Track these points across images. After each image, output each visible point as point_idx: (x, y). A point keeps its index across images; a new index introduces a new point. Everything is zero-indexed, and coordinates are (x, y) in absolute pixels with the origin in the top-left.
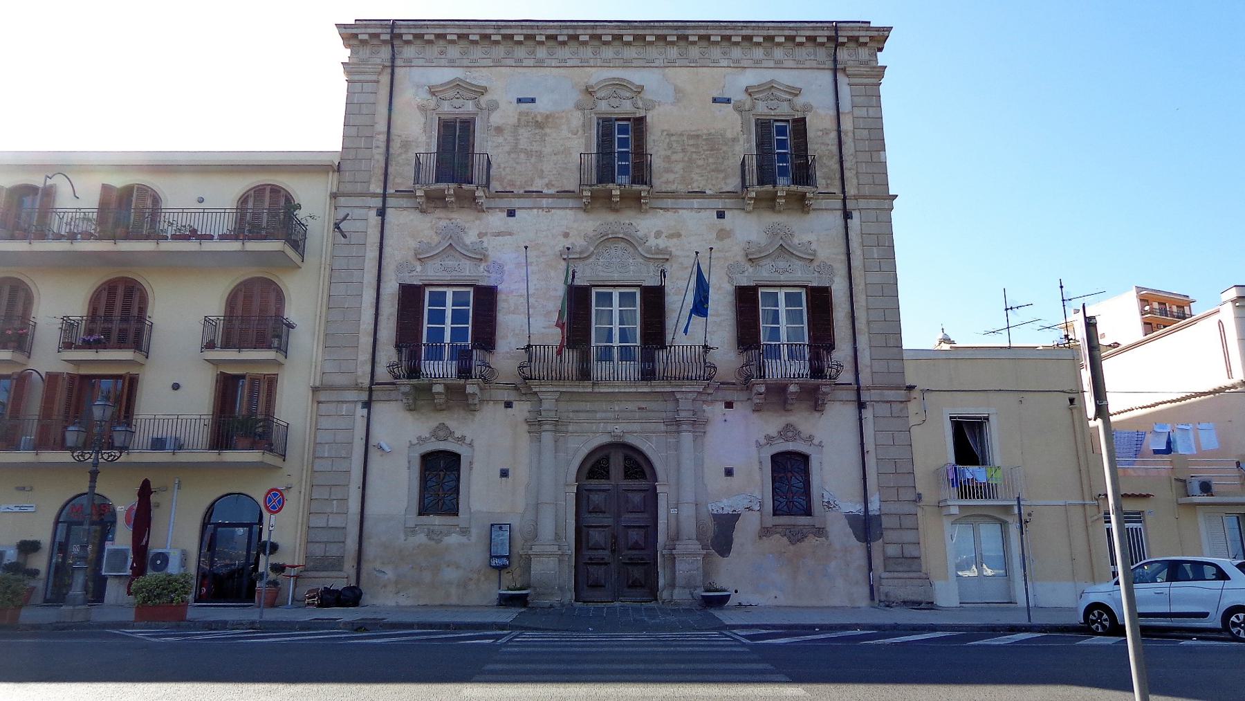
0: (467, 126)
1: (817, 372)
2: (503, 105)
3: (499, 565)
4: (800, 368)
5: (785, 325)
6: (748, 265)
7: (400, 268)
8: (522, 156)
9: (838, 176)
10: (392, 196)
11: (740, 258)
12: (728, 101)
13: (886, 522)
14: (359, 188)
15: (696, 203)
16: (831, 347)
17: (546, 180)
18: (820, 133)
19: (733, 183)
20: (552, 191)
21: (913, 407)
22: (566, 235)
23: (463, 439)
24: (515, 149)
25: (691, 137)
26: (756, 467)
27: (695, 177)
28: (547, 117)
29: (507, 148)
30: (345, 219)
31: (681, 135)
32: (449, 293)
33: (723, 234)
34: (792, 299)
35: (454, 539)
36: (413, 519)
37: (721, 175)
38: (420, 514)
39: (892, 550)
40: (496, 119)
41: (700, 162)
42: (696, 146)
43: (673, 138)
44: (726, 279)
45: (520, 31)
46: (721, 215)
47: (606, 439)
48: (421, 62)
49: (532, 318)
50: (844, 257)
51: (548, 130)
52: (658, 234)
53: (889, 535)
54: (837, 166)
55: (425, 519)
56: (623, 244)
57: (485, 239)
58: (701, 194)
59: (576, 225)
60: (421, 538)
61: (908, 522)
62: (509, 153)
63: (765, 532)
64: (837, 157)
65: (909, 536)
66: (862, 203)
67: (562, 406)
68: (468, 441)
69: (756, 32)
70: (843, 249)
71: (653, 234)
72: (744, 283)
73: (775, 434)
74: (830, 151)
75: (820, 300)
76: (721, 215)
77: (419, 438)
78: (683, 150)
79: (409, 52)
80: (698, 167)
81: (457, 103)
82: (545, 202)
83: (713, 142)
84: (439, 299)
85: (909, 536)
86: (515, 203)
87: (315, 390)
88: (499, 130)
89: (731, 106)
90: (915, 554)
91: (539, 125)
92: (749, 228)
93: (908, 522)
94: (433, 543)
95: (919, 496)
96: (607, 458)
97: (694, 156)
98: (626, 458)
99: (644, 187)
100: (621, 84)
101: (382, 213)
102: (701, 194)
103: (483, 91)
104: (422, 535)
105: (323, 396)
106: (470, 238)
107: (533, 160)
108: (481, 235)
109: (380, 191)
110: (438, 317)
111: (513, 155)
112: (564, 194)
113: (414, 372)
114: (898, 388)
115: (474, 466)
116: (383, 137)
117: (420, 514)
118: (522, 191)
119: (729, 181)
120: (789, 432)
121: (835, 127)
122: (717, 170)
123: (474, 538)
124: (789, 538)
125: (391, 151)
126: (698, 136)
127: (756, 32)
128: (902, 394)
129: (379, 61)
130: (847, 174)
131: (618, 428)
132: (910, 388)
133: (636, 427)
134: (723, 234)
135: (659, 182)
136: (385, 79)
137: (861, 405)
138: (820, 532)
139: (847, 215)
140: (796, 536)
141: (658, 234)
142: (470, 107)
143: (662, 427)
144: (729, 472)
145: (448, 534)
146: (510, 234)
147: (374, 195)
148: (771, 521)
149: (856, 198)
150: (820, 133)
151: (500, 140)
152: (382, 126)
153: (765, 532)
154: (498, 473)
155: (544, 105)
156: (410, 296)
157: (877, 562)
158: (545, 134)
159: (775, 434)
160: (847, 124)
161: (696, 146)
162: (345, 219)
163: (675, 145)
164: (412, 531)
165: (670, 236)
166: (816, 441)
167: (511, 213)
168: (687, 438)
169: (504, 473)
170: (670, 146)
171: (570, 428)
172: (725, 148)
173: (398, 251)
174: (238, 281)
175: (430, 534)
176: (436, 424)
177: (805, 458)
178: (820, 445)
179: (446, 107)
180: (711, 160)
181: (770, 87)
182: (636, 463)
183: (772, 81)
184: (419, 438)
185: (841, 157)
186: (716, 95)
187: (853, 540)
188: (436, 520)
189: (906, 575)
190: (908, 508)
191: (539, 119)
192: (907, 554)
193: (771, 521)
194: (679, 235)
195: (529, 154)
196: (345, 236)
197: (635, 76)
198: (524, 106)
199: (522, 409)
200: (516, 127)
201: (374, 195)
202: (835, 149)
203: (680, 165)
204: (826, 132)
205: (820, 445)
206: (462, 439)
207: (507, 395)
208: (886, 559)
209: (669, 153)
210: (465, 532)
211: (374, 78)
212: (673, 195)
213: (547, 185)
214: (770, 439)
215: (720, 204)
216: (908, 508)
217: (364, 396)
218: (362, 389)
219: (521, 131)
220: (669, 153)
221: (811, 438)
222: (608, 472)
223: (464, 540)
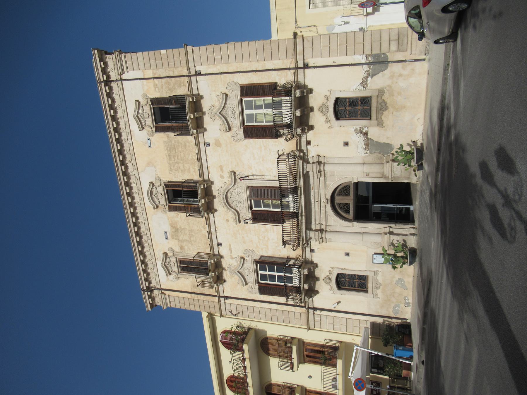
0: (182, 262)
1: (287, 93)
2: (171, 246)
3: (394, 261)
4: (286, 101)
5: (262, 114)
6: (233, 130)
7: (250, 291)
8: (192, 238)
9: (178, 79)
10: (219, 293)
11: (229, 134)
12: (149, 139)
13: (376, 51)
14: (217, 306)
15: (203, 158)
16: (275, 84)
17: (202, 228)
18: (157, 89)
19: (190, 139)
20: (207, 226)
21: (306, 33)
22: (227, 220)
23: (330, 271)
24: (189, 241)
25: (170, 158)
26: (343, 129)
27: (190, 157)
28: (172, 226)
29: (190, 245)
30: (231, 312)
31: (170, 164)
32: (260, 272)
33: (218, 144)
34: (250, 107)
35: (380, 278)
36: (370, 295)
37: (187, 144)
38: (367, 291)
39: (394, 47)
40: (177, 249)
41: (182, 155)
42: (174, 156)
43: (172, 168)
44: (241, 142)
45: (135, 238)
46: (208, 144)
47: (329, 206)
48: (157, 278)
49: (270, 241)
50: (223, 76)
51: (178, 227)
52: (222, 177)
53: (384, 49)
54: (173, 79)
55: (370, 289)
56: (229, 195)
57: (234, 257)
58: (199, 155)
59: (222, 216)
60: (379, 292)
61: (376, 36)
62: (192, 244)
63: (380, 124)
64: (168, 79)
65: (385, 37)
66: (191, 65)
67: (313, 227)
68: (331, 270)
69: (111, 126)
70: (218, 76)
71: (222, 179)
72: (242, 132)
73: (325, 117)
74: (165, 83)
75: (249, 91)
76: (208, 144)
77: (330, 289)
78: (178, 163)
79: (154, 284)
80: (185, 156)
81: (172, 264)
82: (213, 230)
83: (171, 148)
84: (264, 277)
85: (385, 37)
86: (215, 243)
87: (309, 329)
88: (182, 248)
89: (151, 138)
90: (396, 31)
91: (177, 230)
92: (213, 126)
93: (376, 36)
94: (381, 287)
95: (361, 29)
96: (339, 204)
97: (179, 158)
98: (339, 194)
99: (198, 187)
100: (151, 193)
101: (226, 298)
102: (199, 155)
103: (165, 254)
104: (377, 291)
105: (312, 326)
106: (235, 263)
107: (194, 234)
108: (232, 258)
109: (217, 298)
110: (272, 278)
111: (193, 242)
112: (208, 222)
113: (298, 290)
114: (295, 44)
115: (343, 267)
116: (193, 295)
117: (367, 291)
118: (209, 240)
119: (190, 140)
120: (323, 109)
121: (152, 80)
122: (185, 145)
123: (379, 269)
124: (384, 111)
125: (198, 292)
126: (169, 156)
127: (111, 126)
128: (299, 41)
129: (160, 295)
130: (176, 74)
131: (323, 200)
132: (295, 35)
133: (322, 192)
134: (218, 144)
135: (196, 177)
136: (167, 293)
137: (306, 66)
138: (381, 92)
139: (199, 74)
140: (383, 107)
141: (222, 177)
142: (173, 260)
143: (322, 179)
144: (346, 144)
145: (377, 280)
146: (230, 245)
147: (219, 301)
148: (374, 121)
149: (189, 69)
150: (157, 89)
151: (186, 248)
152: (189, 295)
153: (380, 124)
154: (347, 257)
155: (168, 228)
156: (264, 289)
157: (400, 56)
158: (181, 228)
159: (325, 117)
160: (149, 74)
161: (174, 156)
162: (231, 312)
163: (175, 167)
164: (375, 295)
165: (222, 170)
166: (328, 94)
167: (220, 244)
168: (327, 168)
169: (347, 254)
170: (176, 170)
171: (324, 223)
172: (173, 142)
173: (243, 292)
174: (262, 351)
175: (377, 288)
176: (323, 282)
177: (337, 100)
178: (330, 91)
179: (175, 269)
180: (180, 149)
181: (137, 118)
182: (341, 190)
183: (134, 117)
184: (330, 289)
185: (168, 77)
186: (148, 146)
187: (387, 72)
188: (370, 285)
189: (410, 38)
190: (368, 35)
191: (174, 230)
192: (396, 38)
193: (374, 121)
194: (221, 167)
195: (191, 236)
196: (239, 313)
197: (146, 187)
198: (169, 237)
199: (314, 244)
200: (179, 240)
201: (219, 301)
202: (164, 80)
203: (186, 165)
204: (155, 86)
205: (330, 91)
206: (330, 272)
207: (308, 250)
208: (398, 50)
209: (180, 171)
210: (376, 273)
211: (167, 297)
212: (201, 171)
213: (204, 228)
214: (327, 121)
215: (202, 146)
216: (368, 35)
217: (311, 311)
218: (308, 312)
219: (181, 238)
220: (180, 171)
221: (327, 97)
222: (346, 204)
223: (380, 274)
